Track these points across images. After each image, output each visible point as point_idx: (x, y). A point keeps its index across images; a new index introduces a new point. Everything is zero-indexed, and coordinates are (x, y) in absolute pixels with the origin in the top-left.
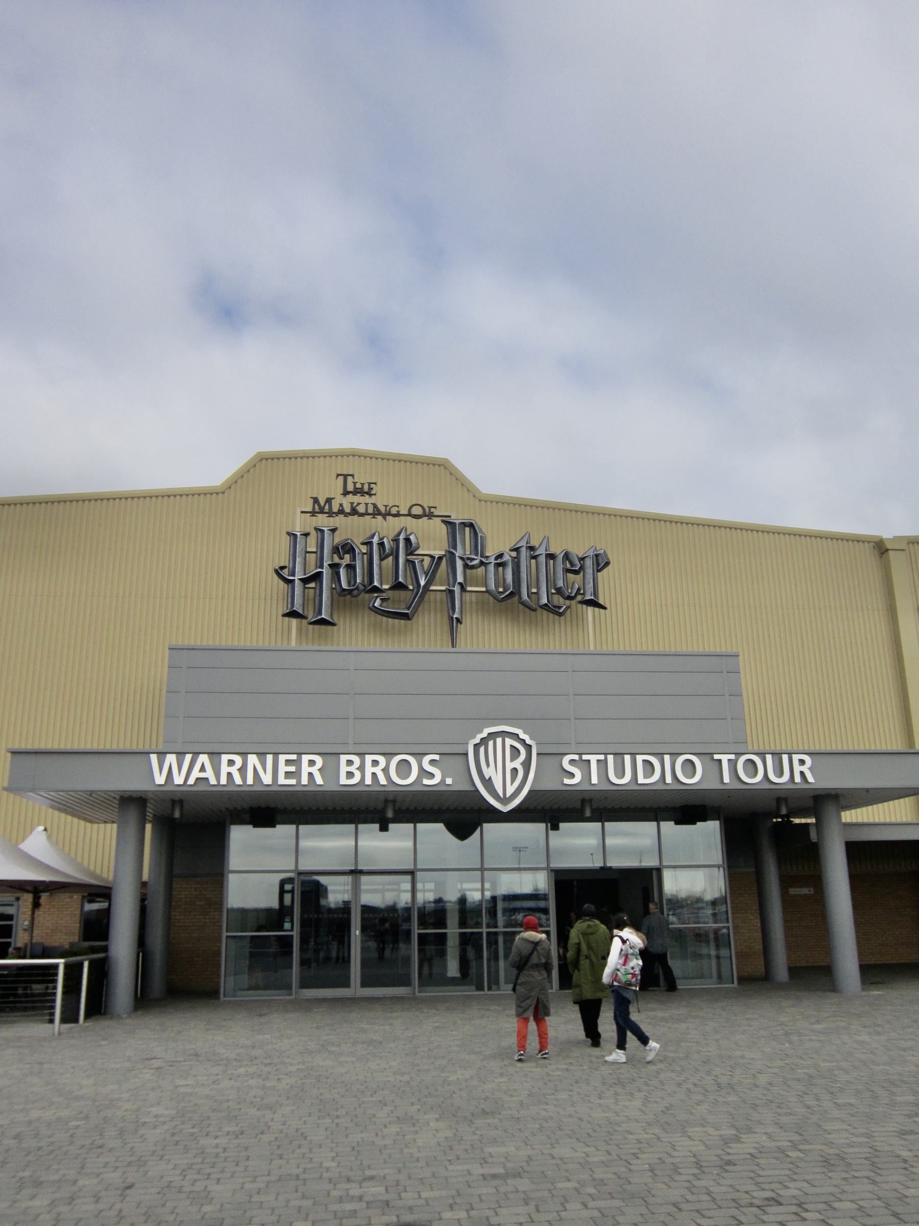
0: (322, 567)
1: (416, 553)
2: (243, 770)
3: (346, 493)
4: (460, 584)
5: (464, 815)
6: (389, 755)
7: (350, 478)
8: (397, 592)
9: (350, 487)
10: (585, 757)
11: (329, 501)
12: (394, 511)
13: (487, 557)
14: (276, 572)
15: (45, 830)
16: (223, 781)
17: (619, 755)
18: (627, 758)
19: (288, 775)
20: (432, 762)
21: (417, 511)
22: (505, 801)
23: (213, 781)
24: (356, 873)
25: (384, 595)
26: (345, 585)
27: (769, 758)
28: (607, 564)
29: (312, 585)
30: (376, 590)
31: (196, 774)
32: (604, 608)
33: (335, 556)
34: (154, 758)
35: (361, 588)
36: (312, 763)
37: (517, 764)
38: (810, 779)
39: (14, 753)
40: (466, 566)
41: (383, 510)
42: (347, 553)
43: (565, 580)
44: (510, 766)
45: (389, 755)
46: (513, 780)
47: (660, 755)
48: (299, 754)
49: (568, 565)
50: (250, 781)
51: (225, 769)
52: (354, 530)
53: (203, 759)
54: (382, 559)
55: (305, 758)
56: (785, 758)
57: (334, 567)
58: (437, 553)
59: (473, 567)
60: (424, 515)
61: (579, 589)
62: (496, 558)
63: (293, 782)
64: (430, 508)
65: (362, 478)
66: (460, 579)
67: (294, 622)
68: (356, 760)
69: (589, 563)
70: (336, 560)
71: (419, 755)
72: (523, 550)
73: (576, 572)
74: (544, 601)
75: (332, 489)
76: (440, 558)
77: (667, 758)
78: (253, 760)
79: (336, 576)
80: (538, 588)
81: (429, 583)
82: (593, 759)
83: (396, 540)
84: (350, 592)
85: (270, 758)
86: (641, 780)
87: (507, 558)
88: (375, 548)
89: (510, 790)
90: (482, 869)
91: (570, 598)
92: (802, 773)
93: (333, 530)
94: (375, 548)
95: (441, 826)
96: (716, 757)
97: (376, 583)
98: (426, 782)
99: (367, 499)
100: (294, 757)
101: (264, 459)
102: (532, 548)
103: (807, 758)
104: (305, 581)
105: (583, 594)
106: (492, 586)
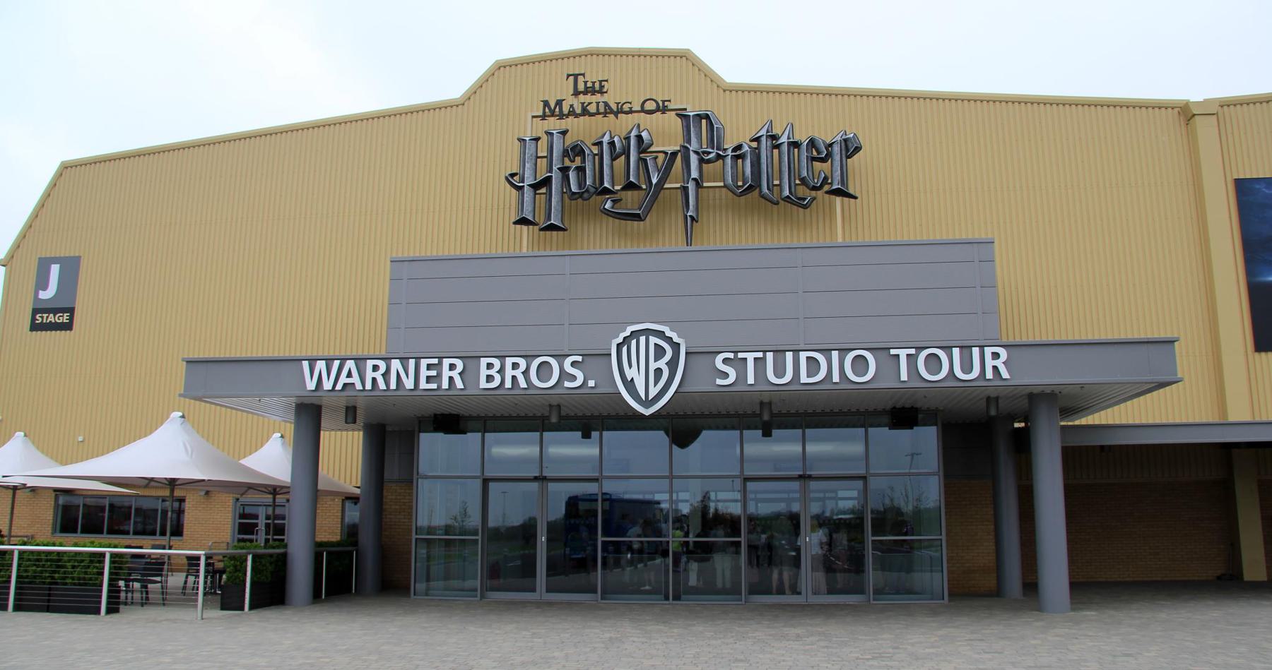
0: (551, 171)
1: (652, 149)
2: (386, 375)
3: (576, 93)
4: (694, 179)
5: (597, 417)
6: (529, 358)
7: (580, 78)
8: (630, 193)
9: (581, 87)
10: (740, 355)
11: (559, 103)
12: (626, 108)
13: (725, 150)
14: (507, 179)
15: (282, 436)
16: (369, 386)
17: (779, 353)
18: (789, 355)
19: (429, 379)
20: (574, 364)
21: (650, 106)
22: (648, 403)
23: (359, 387)
24: (541, 479)
25: (617, 197)
26: (574, 188)
27: (956, 351)
28: (858, 149)
29: (543, 190)
30: (606, 191)
31: (344, 379)
32: (855, 198)
33: (566, 159)
34: (306, 364)
35: (592, 190)
36: (452, 367)
37: (662, 364)
38: (1005, 375)
39: (190, 362)
40: (701, 161)
41: (614, 107)
42: (577, 155)
43: (810, 169)
44: (653, 366)
45: (529, 358)
46: (655, 384)
47: (826, 352)
48: (441, 358)
49: (815, 153)
50: (393, 386)
51: (370, 374)
52: (582, 130)
53: (350, 364)
54: (613, 159)
55: (446, 362)
56: (976, 351)
57: (564, 170)
58: (670, 149)
59: (709, 161)
60: (658, 110)
61: (826, 178)
62: (734, 150)
63: (434, 386)
64: (663, 102)
65: (592, 77)
66: (694, 174)
67: (525, 228)
68: (496, 362)
69: (836, 149)
70: (567, 163)
71: (560, 357)
72: (764, 139)
73: (823, 160)
74: (786, 193)
75: (562, 91)
76: (674, 154)
77: (835, 354)
78: (396, 365)
79: (566, 179)
80: (781, 180)
81: (662, 181)
82: (750, 357)
83: (628, 138)
84: (580, 195)
85: (412, 362)
86: (804, 379)
87: (746, 148)
88: (605, 147)
89: (653, 392)
90: (671, 477)
91: (815, 188)
92: (995, 368)
93: (564, 133)
94: (605, 147)
95: (662, 433)
96: (893, 352)
97: (606, 185)
98: (567, 384)
99: (598, 98)
100: (435, 361)
101: (502, 67)
102: (774, 137)
103: (1003, 353)
104: (535, 187)
105: (831, 184)
106: (730, 181)
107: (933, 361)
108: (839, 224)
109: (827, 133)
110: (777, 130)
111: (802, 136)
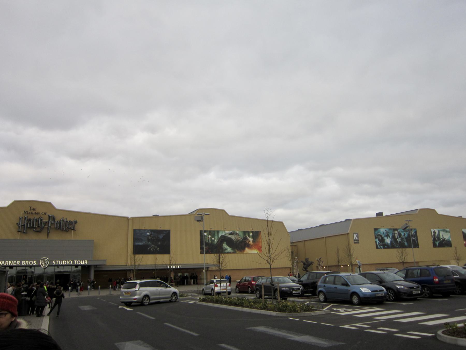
52: (31, 217)
57: (27, 223)
58: (46, 221)
75: (28, 209)
78: (10, 262)
82: (57, 261)
107: (79, 262)
108: (72, 236)
109: (72, 220)
110: (64, 219)
111: (68, 220)
